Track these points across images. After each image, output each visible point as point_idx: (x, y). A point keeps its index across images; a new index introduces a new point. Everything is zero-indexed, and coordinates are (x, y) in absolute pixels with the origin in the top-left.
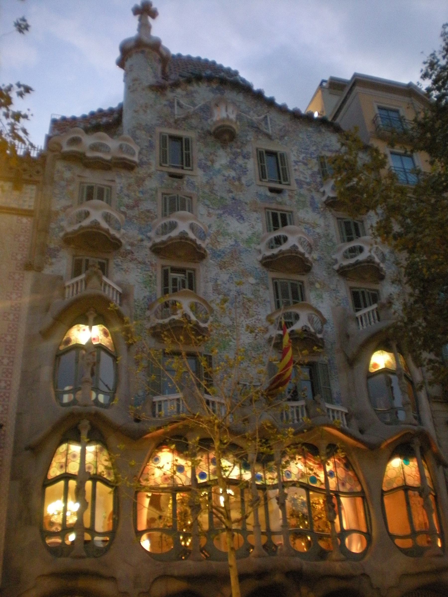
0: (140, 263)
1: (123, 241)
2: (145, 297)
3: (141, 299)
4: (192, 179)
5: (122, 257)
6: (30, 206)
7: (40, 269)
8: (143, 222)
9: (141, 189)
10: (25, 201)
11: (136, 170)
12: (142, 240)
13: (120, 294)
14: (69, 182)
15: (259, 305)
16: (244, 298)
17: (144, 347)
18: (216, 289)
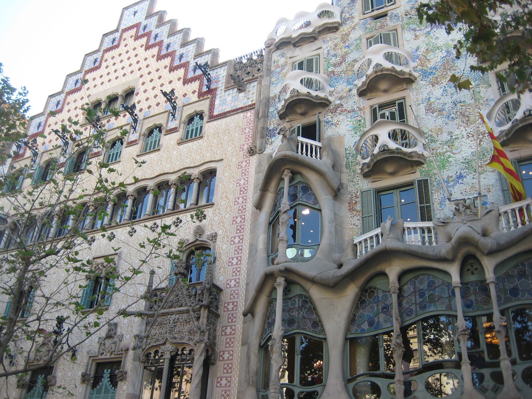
0: (349, 112)
1: (331, 99)
2: (355, 143)
3: (352, 146)
4: (395, 12)
5: (332, 113)
6: (252, 101)
7: (261, 151)
8: (351, 73)
9: (347, 44)
10: (248, 99)
11: (341, 29)
12: (350, 90)
13: (320, 148)
14: (283, 67)
15: (481, 107)
16: (462, 106)
17: (357, 192)
18: (430, 109)
